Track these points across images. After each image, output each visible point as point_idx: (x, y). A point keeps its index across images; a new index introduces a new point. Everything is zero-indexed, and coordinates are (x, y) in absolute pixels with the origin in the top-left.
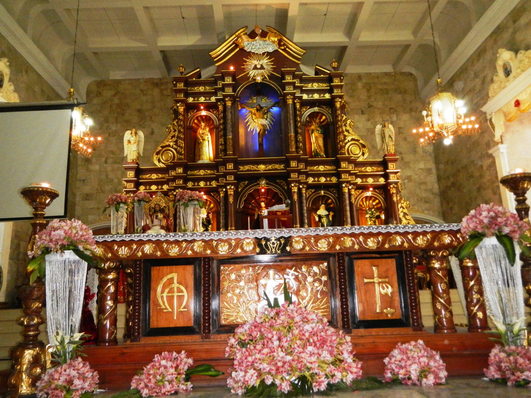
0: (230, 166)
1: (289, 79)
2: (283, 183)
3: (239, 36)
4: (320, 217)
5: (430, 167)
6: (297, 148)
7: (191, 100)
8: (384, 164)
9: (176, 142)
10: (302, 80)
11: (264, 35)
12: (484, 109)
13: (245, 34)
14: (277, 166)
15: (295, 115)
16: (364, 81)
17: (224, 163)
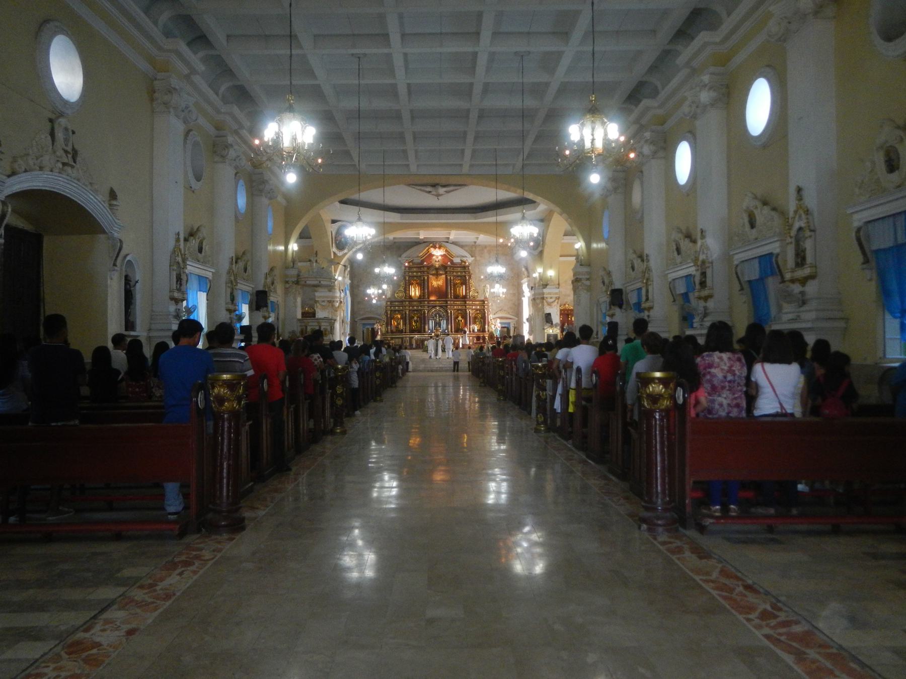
0: (427, 303)
1: (448, 268)
2: (445, 308)
3: (429, 248)
4: (459, 321)
5: (514, 292)
6: (451, 295)
7: (410, 273)
8: (483, 301)
9: (405, 289)
10: (454, 267)
11: (440, 248)
12: (523, 281)
13: (432, 247)
14: (443, 302)
15: (450, 282)
16: (488, 248)
17: (425, 301)
